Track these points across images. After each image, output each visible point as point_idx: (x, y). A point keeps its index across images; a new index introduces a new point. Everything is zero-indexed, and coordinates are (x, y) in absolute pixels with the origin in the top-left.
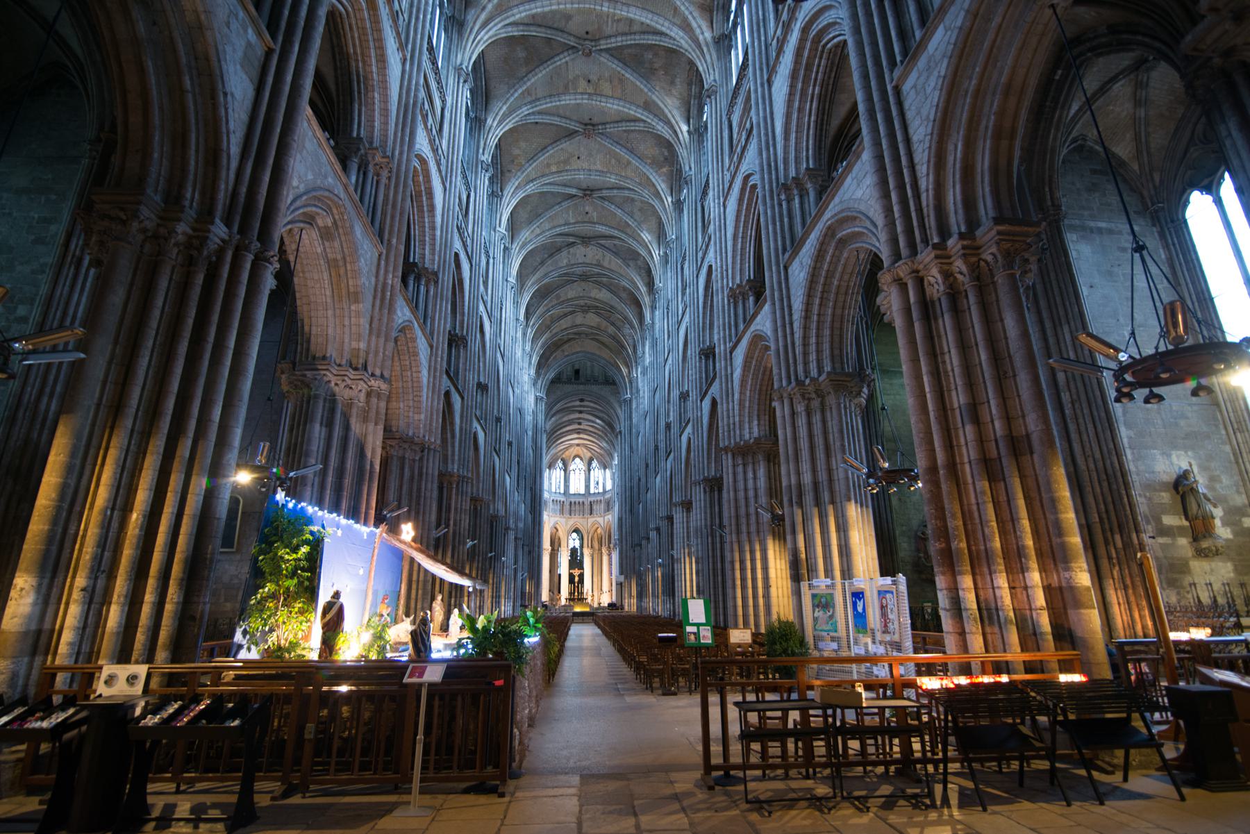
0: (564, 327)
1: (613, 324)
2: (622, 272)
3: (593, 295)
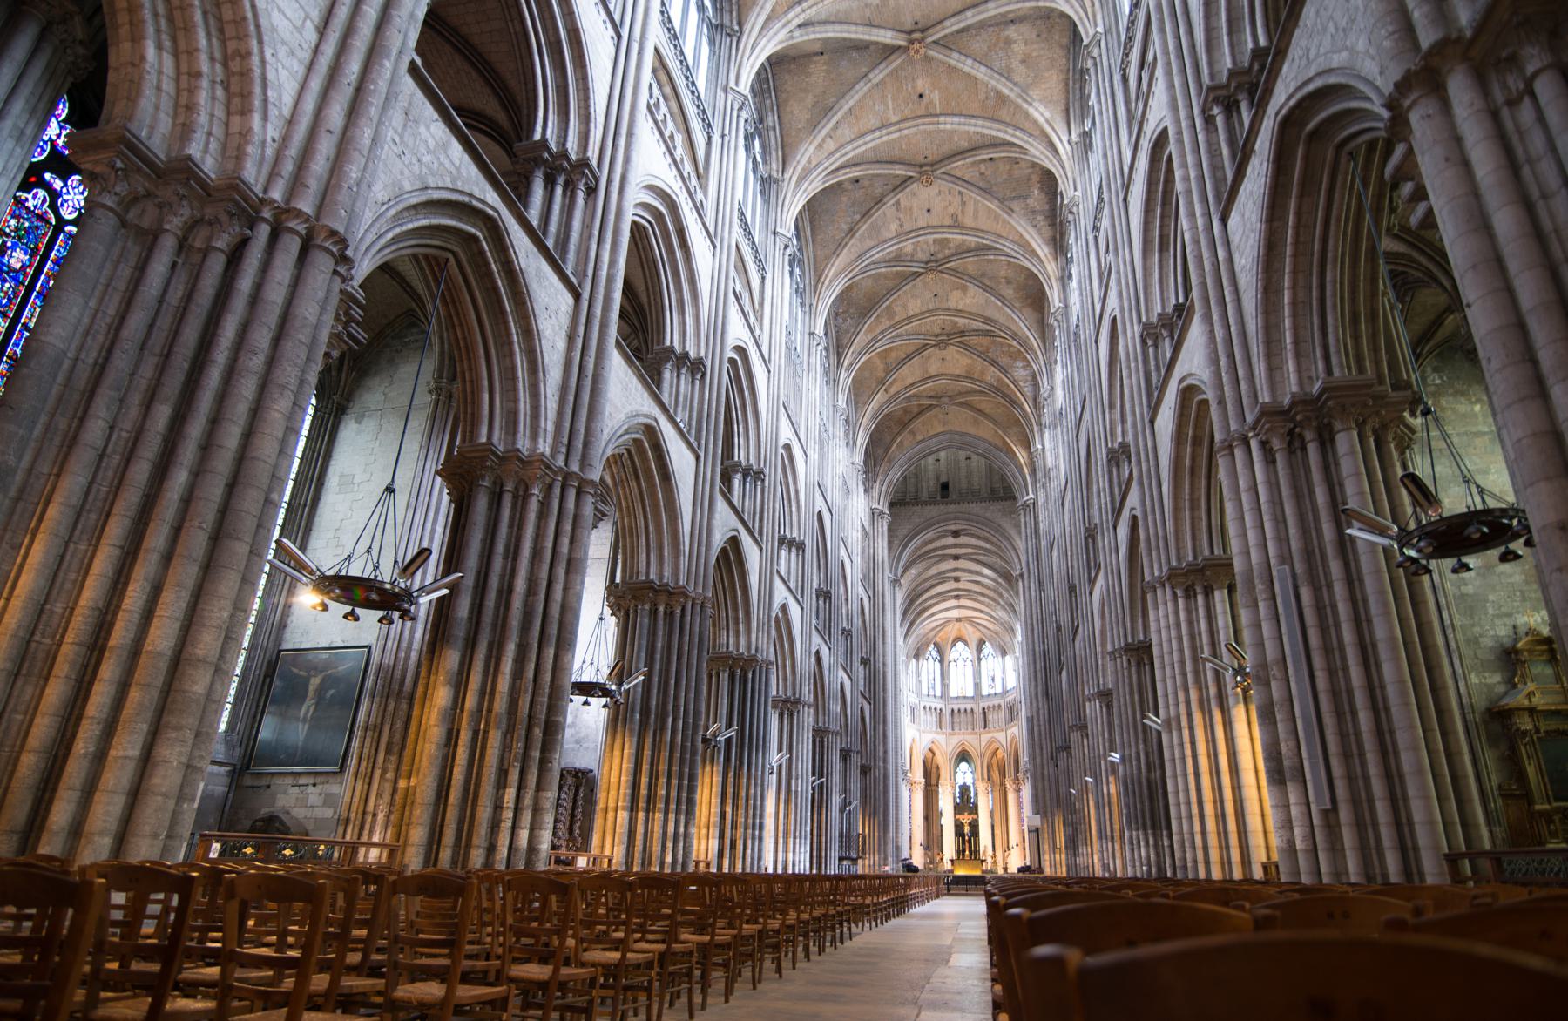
0: (910, 381)
1: (994, 363)
2: (999, 229)
3: (952, 304)
